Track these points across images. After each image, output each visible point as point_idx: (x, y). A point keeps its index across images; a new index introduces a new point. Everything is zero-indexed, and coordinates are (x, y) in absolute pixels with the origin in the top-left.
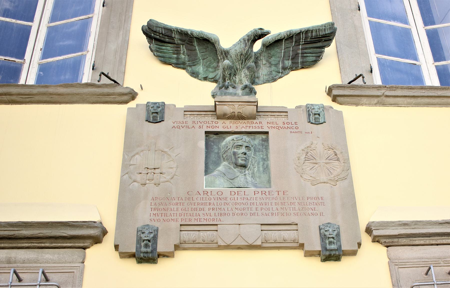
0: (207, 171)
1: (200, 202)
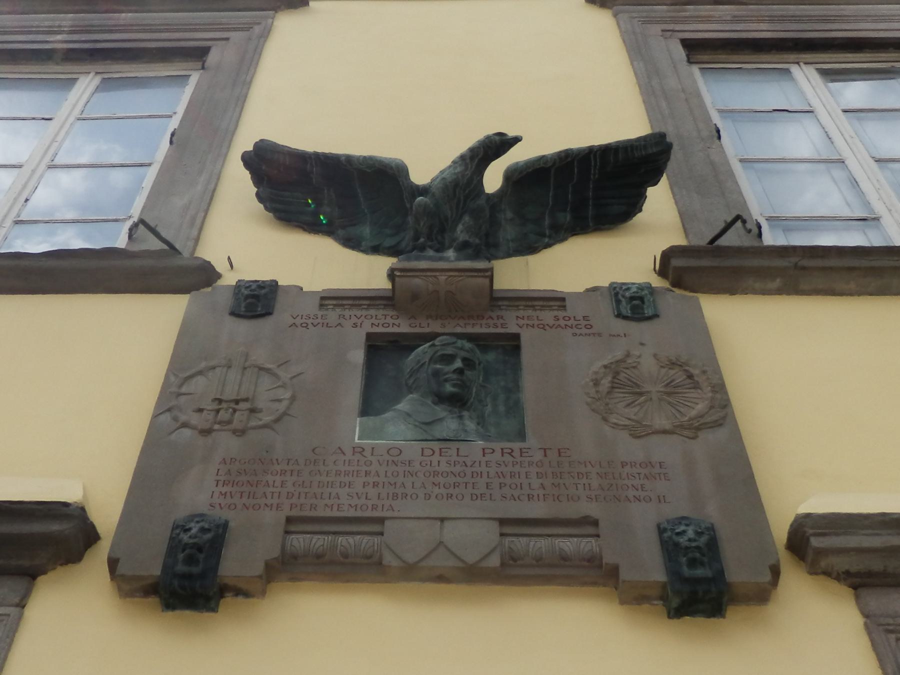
0: (367, 409)
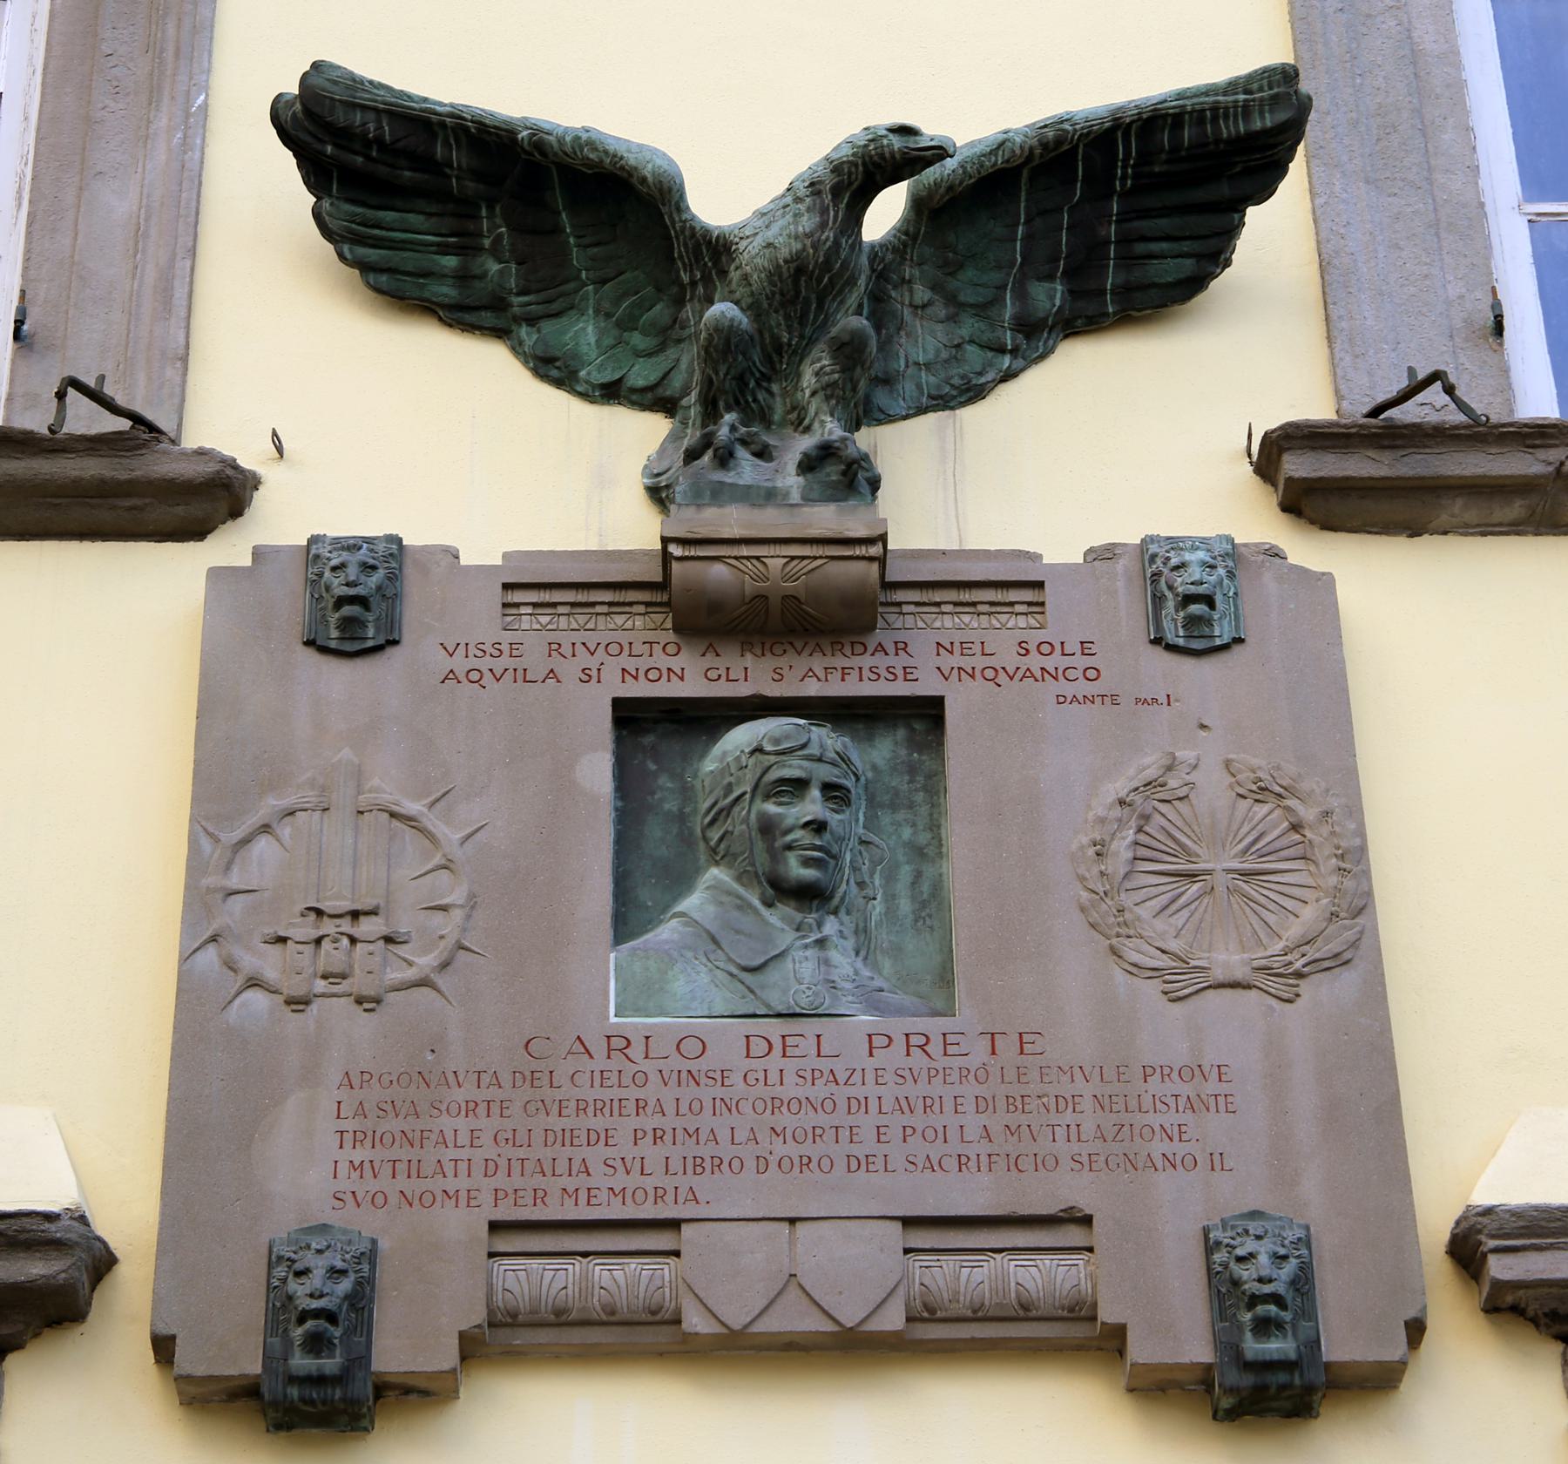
1: (590, 1095)
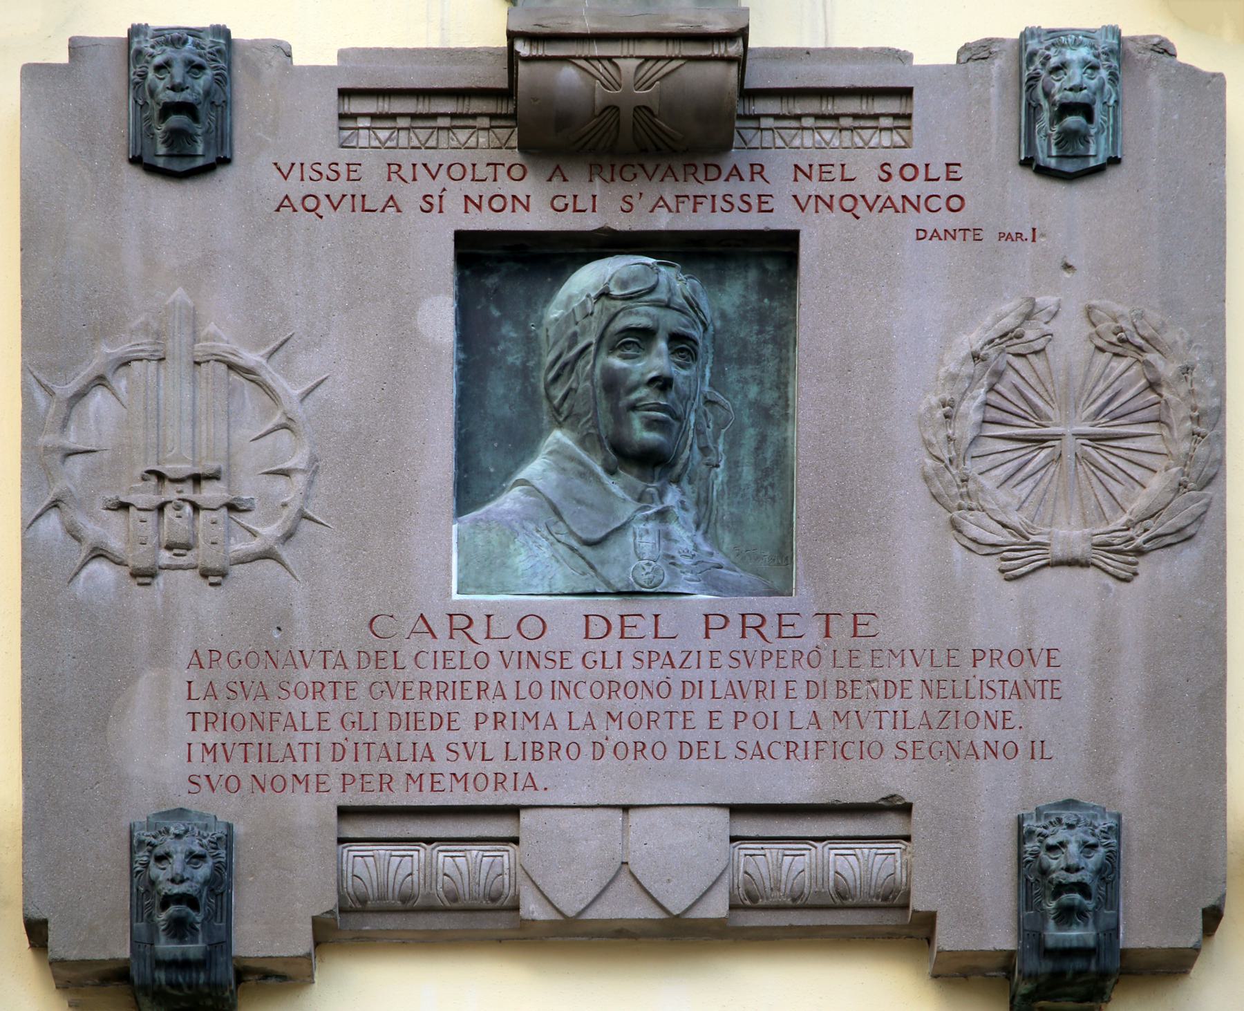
0: (470, 490)
